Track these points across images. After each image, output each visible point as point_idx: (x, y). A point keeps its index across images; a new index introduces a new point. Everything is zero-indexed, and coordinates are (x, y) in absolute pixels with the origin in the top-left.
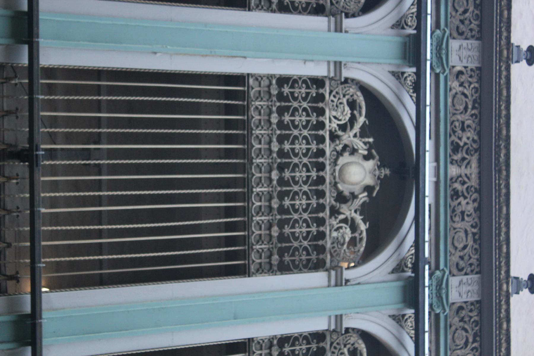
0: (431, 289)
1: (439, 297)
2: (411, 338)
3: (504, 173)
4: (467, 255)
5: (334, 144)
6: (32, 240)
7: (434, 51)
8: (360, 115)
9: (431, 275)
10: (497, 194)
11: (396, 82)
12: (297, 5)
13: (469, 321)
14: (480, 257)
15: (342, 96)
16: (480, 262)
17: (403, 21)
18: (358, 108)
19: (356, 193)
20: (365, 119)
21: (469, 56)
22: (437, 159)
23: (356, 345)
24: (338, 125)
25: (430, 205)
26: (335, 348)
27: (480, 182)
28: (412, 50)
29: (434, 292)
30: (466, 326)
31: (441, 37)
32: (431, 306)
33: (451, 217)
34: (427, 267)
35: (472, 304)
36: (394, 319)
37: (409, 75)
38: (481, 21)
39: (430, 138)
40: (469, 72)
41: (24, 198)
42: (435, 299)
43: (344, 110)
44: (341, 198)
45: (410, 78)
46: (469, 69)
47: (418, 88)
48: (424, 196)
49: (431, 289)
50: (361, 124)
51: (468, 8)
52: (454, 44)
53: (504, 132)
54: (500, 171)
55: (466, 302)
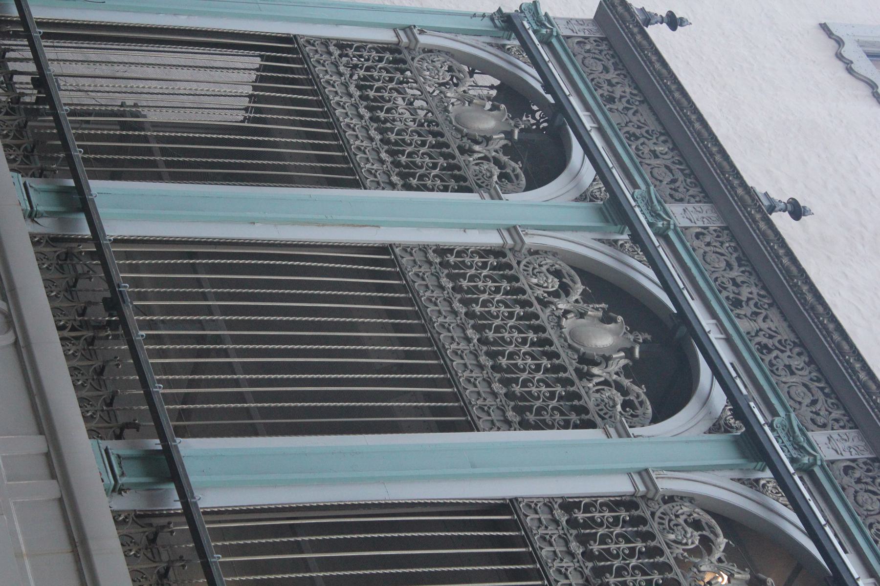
0: (780, 441)
1: (800, 448)
2: (786, 506)
3: (820, 309)
4: (823, 408)
5: (691, 574)
6: (191, 522)
7: (645, 212)
8: (717, 536)
9: (773, 430)
10: (824, 333)
11: (612, 248)
12: (615, 552)
13: (873, 482)
14: (846, 411)
15: (673, 517)
16: (849, 416)
17: (722, 422)
18: (706, 528)
19: (607, 355)
20: (726, 540)
21: (850, 447)
22: (713, 315)
23: (695, 515)
24: (683, 550)
25: (732, 364)
26: (605, 414)
27: (796, 334)
28: (614, 211)
29: (787, 443)
30: (870, 488)
31: (788, 426)
32: (793, 460)
33: (772, 371)
34: (752, 404)
35: (865, 463)
36: (743, 483)
37: (768, 482)
38: (845, 409)
39: (846, 552)
40: (862, 465)
41: (134, 380)
42: (793, 452)
43: (686, 532)
44: (587, 360)
45: (770, 485)
46: (860, 462)
47: (637, 238)
48: (706, 334)
49: (780, 441)
50: (723, 547)
51: (816, 398)
52: (818, 437)
53: (846, 347)
54: (813, 308)
55: (854, 461)
